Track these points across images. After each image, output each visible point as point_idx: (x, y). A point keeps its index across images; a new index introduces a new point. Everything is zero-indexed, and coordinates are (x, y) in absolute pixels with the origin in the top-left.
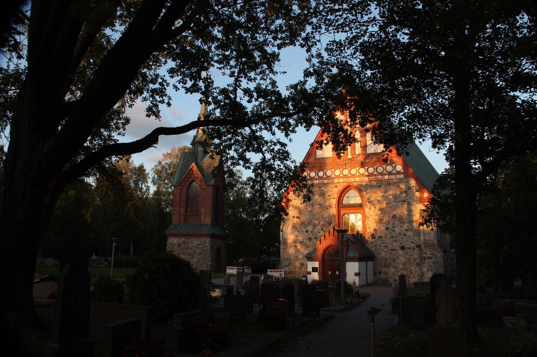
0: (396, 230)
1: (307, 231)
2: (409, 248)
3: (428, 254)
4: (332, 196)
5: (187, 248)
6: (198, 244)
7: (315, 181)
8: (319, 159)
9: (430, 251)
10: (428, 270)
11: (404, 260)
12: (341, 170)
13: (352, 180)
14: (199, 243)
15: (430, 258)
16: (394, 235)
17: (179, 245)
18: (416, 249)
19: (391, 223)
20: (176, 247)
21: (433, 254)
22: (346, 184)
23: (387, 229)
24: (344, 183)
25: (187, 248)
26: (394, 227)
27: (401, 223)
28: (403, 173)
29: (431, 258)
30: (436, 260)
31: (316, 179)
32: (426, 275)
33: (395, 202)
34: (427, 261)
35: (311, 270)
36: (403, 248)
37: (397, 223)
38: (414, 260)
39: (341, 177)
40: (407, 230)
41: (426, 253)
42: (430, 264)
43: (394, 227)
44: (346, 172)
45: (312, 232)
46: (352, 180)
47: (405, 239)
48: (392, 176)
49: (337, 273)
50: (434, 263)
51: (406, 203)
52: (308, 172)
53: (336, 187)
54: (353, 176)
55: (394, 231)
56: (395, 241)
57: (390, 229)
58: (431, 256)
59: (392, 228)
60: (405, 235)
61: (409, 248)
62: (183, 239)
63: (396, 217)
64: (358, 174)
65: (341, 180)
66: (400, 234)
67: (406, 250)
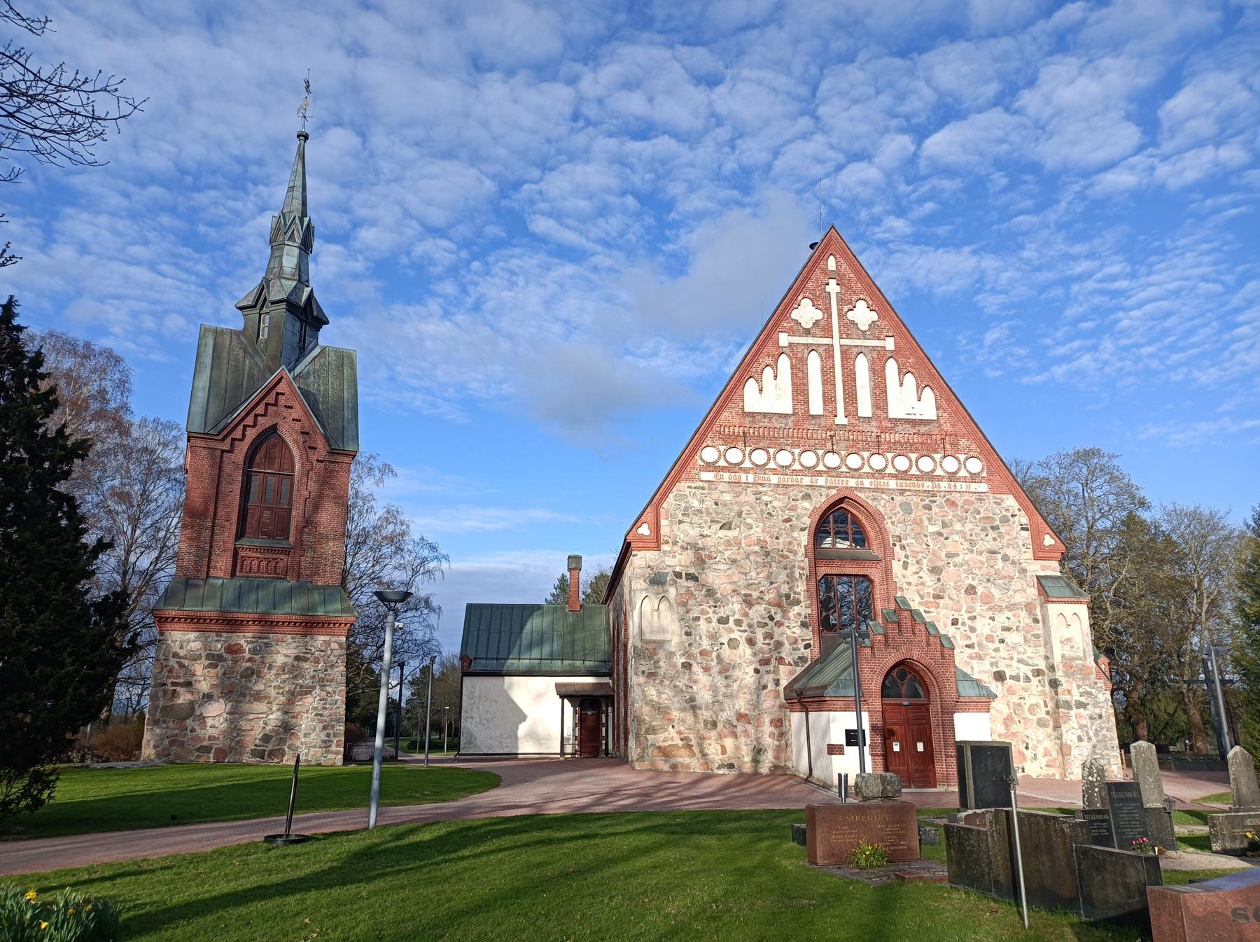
0: (978, 624)
3: (1076, 696)
4: (795, 521)
7: (743, 476)
8: (752, 415)
9: (1079, 687)
10: (1080, 739)
11: (1006, 711)
12: (820, 452)
13: (852, 483)
16: (974, 640)
19: (964, 608)
21: (1089, 694)
22: (834, 492)
24: (829, 488)
26: (975, 618)
27: (990, 609)
29: (1081, 705)
30: (1097, 711)
31: (746, 471)
32: (1075, 752)
33: (972, 552)
34: (1074, 712)
35: (843, 741)
36: (1000, 676)
37: (979, 608)
38: (1032, 709)
39: (820, 473)
40: (1008, 629)
41: (1069, 692)
42: (1083, 722)
43: (975, 618)
44: (832, 460)
46: (852, 483)
47: (1003, 653)
48: (958, 484)
49: (920, 747)
51: (999, 556)
52: (722, 448)
53: (807, 497)
54: (855, 473)
55: (973, 629)
56: (979, 657)
57: (964, 624)
58: (1083, 699)
59: (969, 623)
60: (1002, 641)
63: (975, 593)
64: (866, 469)
65: (821, 481)
66: (990, 638)
67: (1009, 682)
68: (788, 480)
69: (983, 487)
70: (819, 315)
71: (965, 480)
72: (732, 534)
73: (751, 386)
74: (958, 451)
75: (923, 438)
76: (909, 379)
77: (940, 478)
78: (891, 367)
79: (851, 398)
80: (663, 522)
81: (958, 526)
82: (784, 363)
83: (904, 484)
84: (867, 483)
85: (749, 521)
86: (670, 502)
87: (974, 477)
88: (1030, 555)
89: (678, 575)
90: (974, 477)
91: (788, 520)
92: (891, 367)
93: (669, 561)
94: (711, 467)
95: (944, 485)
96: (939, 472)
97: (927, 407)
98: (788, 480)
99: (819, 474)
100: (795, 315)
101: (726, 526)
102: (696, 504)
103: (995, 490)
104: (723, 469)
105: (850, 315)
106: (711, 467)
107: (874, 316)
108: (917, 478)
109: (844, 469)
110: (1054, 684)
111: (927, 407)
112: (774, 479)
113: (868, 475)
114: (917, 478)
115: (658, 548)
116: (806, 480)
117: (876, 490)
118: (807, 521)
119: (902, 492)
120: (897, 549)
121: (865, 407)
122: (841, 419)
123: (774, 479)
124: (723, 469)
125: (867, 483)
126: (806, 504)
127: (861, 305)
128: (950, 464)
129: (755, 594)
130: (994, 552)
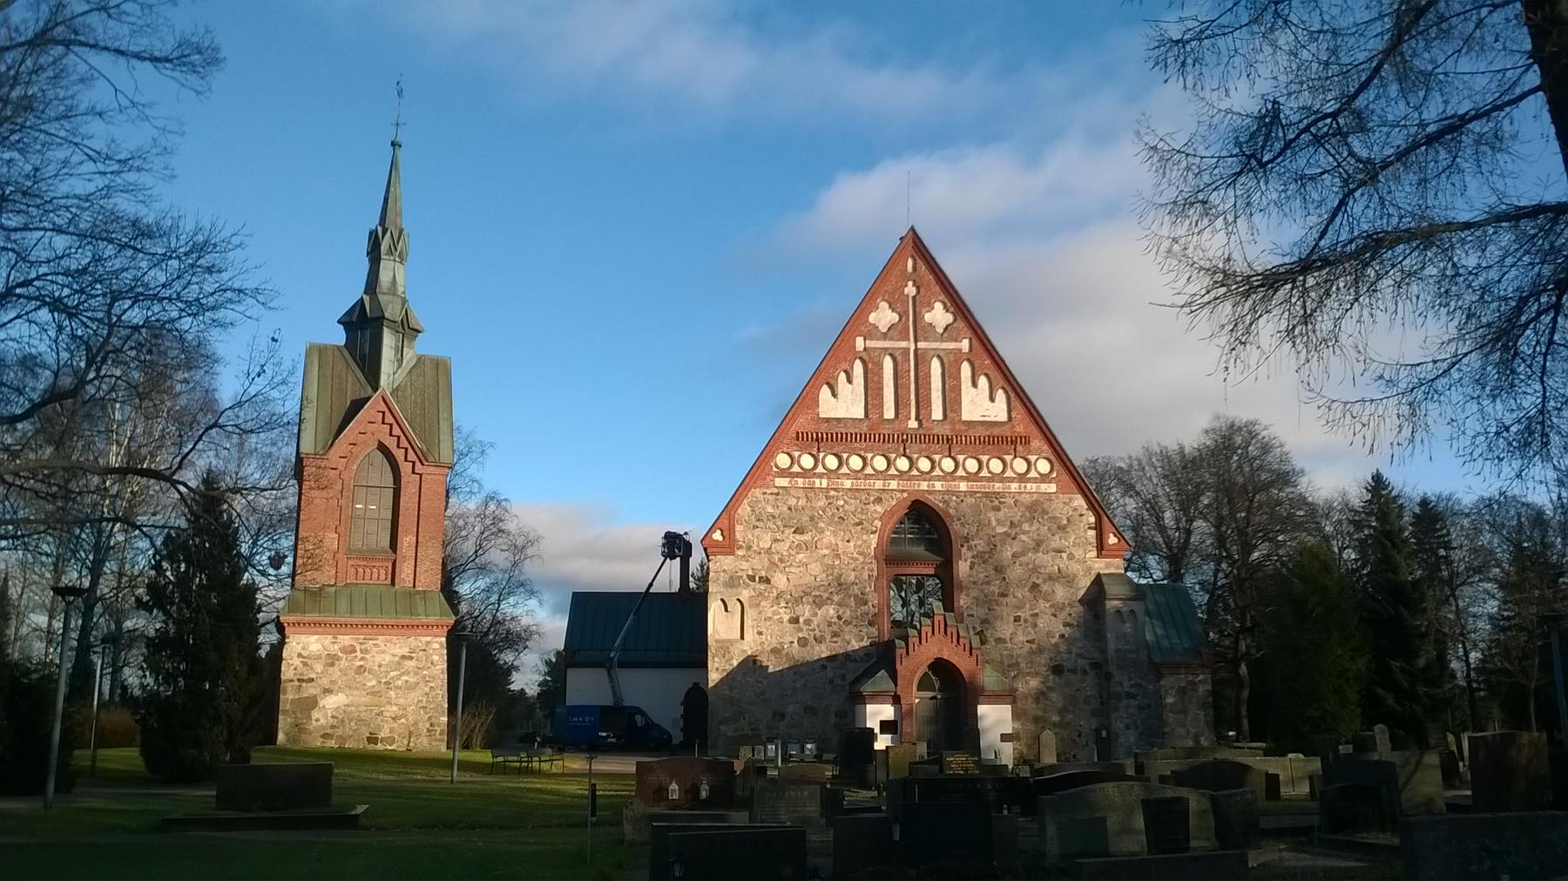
1: (795, 620)
2: (1073, 671)
5: (361, 670)
6: (403, 657)
7: (817, 481)
8: (828, 420)
10: (1127, 727)
14: (405, 651)
15: (1130, 696)
17: (332, 660)
18: (1092, 673)
20: (319, 668)
23: (1017, 619)
25: (361, 670)
28: (1057, 481)
29: (1133, 697)
30: (1146, 701)
31: (821, 476)
32: (1122, 739)
34: (1125, 702)
39: (893, 477)
41: (1121, 683)
42: (1132, 711)
45: (808, 622)
46: (924, 486)
50: (1140, 708)
53: (879, 500)
61: (1073, 671)
62: (346, 640)
65: (894, 484)
68: (861, 484)
69: (1052, 488)
70: (895, 317)
71: (1034, 480)
72: (806, 537)
73: (825, 392)
74: (1030, 452)
75: (994, 440)
76: (983, 382)
77: (1011, 480)
78: (966, 369)
79: (923, 403)
80: (738, 528)
81: (1026, 527)
82: (858, 368)
83: (976, 486)
84: (938, 486)
85: (822, 525)
86: (744, 510)
87: (1044, 478)
88: (1094, 553)
89: (752, 578)
90: (1044, 478)
91: (860, 524)
92: (966, 369)
93: (745, 565)
94: (783, 473)
95: (1014, 486)
96: (1009, 473)
97: (997, 410)
98: (861, 484)
99: (894, 478)
100: (872, 318)
101: (799, 531)
102: (770, 509)
103: (1062, 490)
104: (797, 475)
105: (928, 317)
106: (783, 473)
107: (949, 318)
108: (988, 480)
109: (915, 472)
110: (1108, 676)
111: (997, 410)
112: (848, 484)
113: (939, 478)
114: (988, 480)
115: (733, 553)
116: (879, 484)
117: (947, 492)
118: (878, 523)
119: (972, 494)
120: (964, 550)
121: (937, 414)
122: (913, 424)
123: (848, 484)
124: (797, 475)
125: (938, 486)
126: (879, 508)
127: (938, 306)
128: (1020, 465)
129: (826, 595)
130: (1060, 552)
